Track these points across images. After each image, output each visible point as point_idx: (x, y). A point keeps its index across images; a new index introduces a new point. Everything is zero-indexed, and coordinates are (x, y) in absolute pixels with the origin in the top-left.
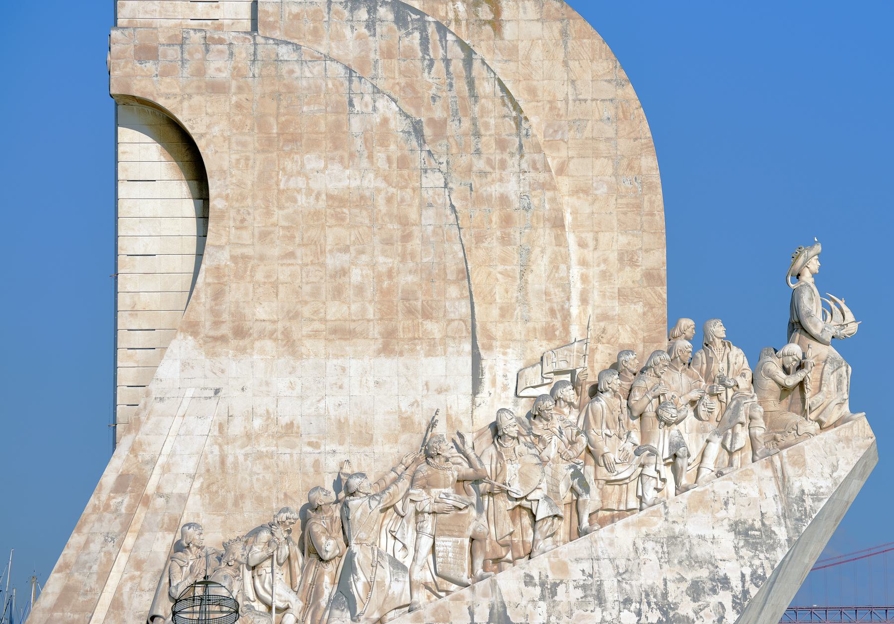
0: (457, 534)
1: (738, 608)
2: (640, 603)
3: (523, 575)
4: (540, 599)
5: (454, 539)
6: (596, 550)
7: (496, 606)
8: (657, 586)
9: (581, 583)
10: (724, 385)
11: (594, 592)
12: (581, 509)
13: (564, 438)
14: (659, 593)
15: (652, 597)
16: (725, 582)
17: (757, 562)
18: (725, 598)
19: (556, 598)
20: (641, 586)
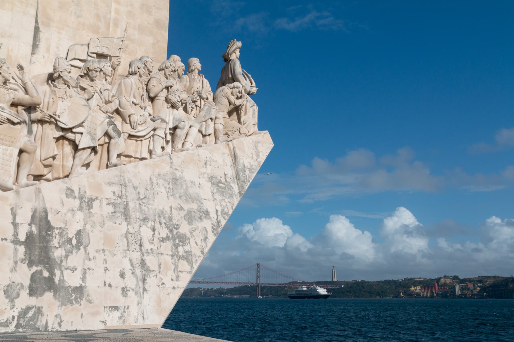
0: (8, 143)
1: (215, 232)
2: (154, 222)
3: (65, 188)
4: (79, 210)
5: (4, 147)
6: (124, 179)
7: (38, 211)
8: (166, 211)
9: (112, 201)
10: (201, 97)
11: (122, 210)
12: (112, 148)
13: (102, 97)
14: (167, 215)
15: (162, 218)
16: (207, 213)
17: (224, 204)
18: (207, 224)
19: (91, 210)
20: (155, 210)
